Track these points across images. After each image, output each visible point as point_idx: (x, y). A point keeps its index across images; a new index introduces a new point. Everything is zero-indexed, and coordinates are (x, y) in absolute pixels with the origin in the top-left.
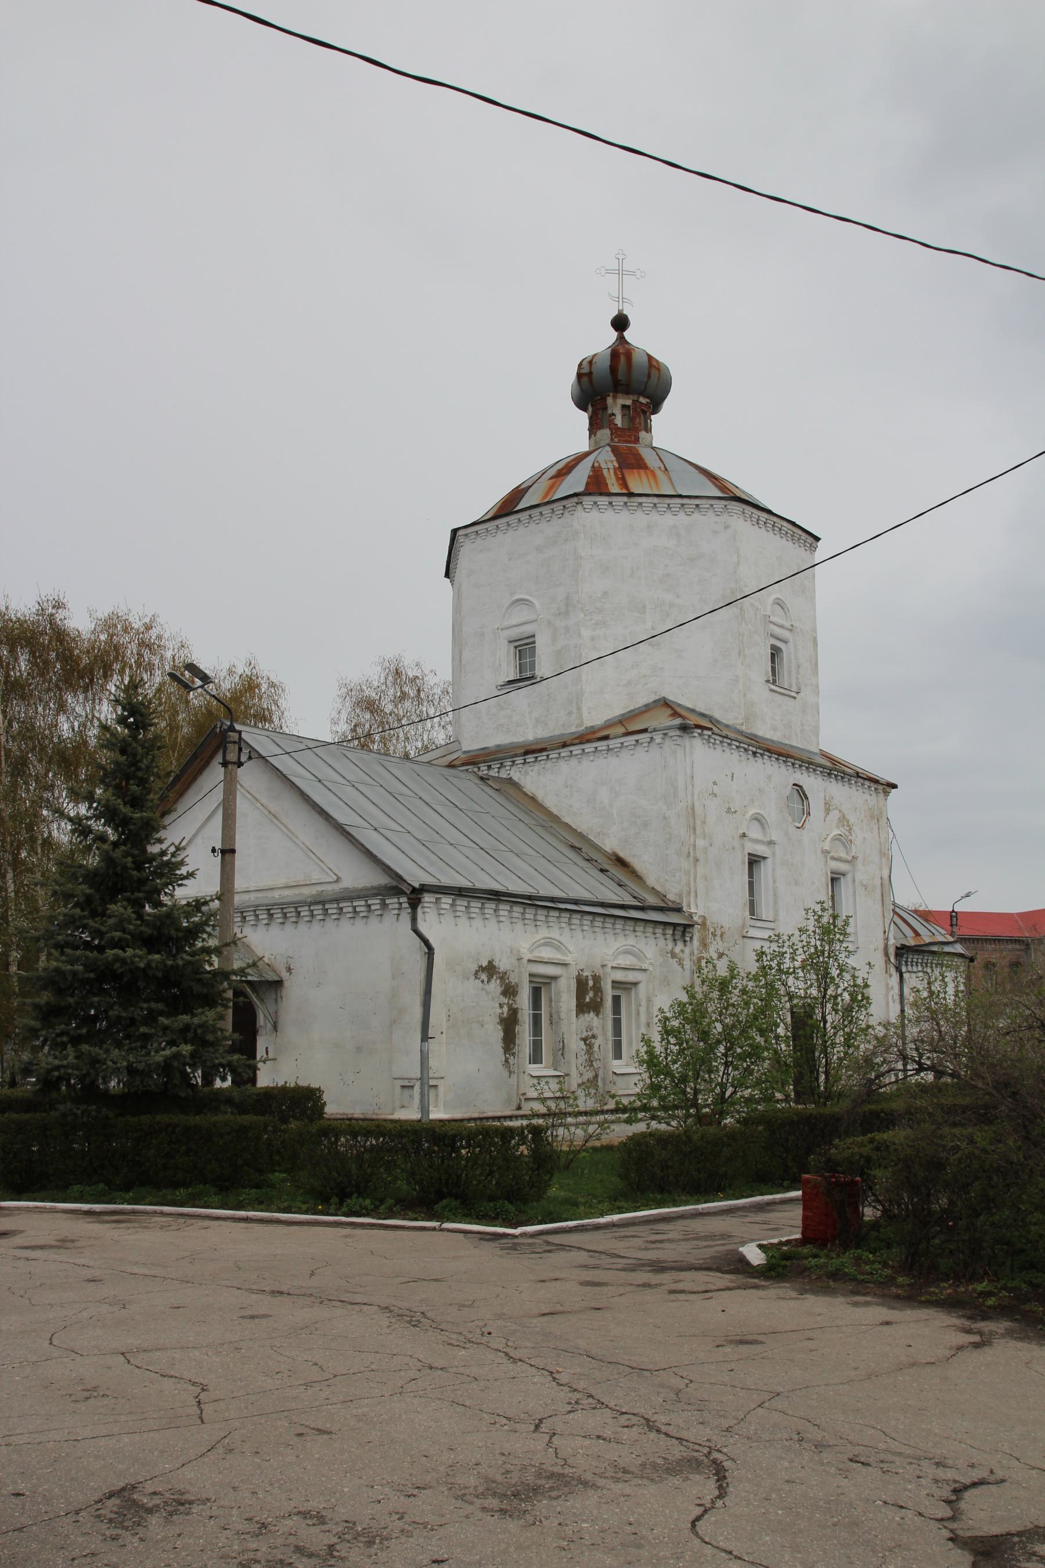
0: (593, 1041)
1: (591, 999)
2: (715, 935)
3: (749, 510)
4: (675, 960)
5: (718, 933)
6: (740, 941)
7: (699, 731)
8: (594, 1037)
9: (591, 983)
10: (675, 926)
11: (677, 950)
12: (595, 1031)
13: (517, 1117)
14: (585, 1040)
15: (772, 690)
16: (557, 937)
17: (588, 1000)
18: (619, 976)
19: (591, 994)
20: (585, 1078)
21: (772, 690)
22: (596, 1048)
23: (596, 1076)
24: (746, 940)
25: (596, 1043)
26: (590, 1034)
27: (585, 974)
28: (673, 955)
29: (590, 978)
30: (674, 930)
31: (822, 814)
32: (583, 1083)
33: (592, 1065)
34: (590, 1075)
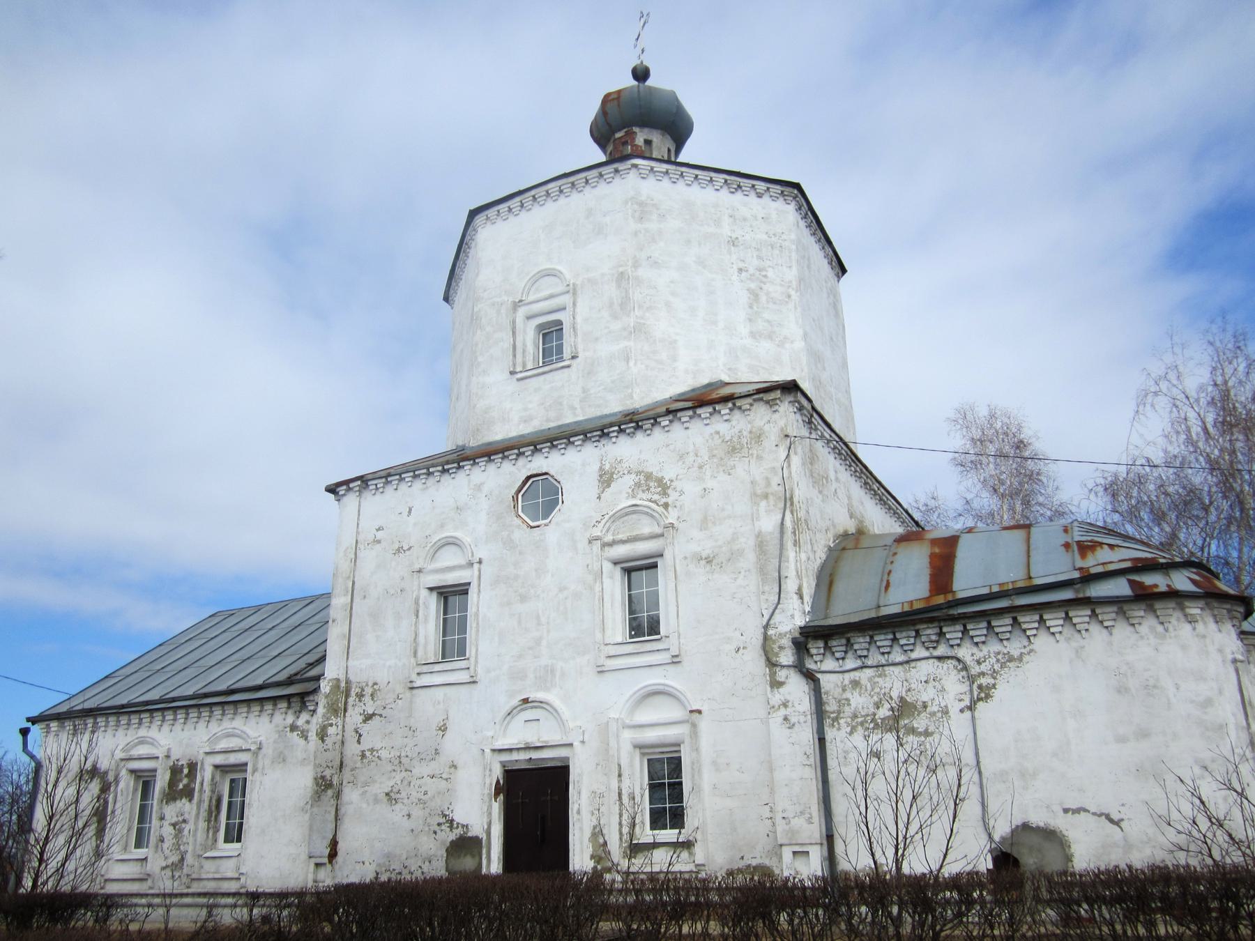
0: (183, 825)
1: (184, 786)
2: (362, 696)
3: (492, 212)
4: (295, 733)
5: (368, 691)
6: (408, 694)
7: (344, 487)
8: (184, 821)
9: (186, 771)
10: (288, 698)
11: (300, 722)
12: (186, 816)
13: (187, 895)
14: (174, 825)
15: (519, 380)
16: (145, 735)
17: (181, 786)
18: (219, 759)
19: (185, 781)
20: (170, 862)
21: (519, 380)
22: (186, 832)
23: (182, 859)
24: (415, 691)
25: (187, 827)
26: (181, 819)
27: (180, 763)
28: (293, 728)
29: (185, 766)
30: (289, 703)
31: (595, 491)
32: (167, 867)
33: (179, 849)
34: (174, 858)
